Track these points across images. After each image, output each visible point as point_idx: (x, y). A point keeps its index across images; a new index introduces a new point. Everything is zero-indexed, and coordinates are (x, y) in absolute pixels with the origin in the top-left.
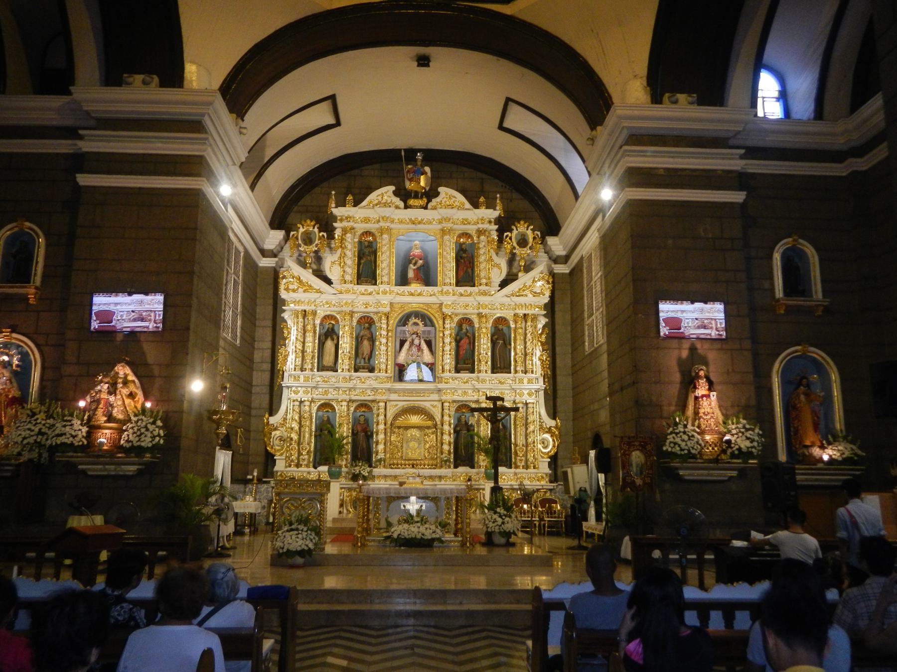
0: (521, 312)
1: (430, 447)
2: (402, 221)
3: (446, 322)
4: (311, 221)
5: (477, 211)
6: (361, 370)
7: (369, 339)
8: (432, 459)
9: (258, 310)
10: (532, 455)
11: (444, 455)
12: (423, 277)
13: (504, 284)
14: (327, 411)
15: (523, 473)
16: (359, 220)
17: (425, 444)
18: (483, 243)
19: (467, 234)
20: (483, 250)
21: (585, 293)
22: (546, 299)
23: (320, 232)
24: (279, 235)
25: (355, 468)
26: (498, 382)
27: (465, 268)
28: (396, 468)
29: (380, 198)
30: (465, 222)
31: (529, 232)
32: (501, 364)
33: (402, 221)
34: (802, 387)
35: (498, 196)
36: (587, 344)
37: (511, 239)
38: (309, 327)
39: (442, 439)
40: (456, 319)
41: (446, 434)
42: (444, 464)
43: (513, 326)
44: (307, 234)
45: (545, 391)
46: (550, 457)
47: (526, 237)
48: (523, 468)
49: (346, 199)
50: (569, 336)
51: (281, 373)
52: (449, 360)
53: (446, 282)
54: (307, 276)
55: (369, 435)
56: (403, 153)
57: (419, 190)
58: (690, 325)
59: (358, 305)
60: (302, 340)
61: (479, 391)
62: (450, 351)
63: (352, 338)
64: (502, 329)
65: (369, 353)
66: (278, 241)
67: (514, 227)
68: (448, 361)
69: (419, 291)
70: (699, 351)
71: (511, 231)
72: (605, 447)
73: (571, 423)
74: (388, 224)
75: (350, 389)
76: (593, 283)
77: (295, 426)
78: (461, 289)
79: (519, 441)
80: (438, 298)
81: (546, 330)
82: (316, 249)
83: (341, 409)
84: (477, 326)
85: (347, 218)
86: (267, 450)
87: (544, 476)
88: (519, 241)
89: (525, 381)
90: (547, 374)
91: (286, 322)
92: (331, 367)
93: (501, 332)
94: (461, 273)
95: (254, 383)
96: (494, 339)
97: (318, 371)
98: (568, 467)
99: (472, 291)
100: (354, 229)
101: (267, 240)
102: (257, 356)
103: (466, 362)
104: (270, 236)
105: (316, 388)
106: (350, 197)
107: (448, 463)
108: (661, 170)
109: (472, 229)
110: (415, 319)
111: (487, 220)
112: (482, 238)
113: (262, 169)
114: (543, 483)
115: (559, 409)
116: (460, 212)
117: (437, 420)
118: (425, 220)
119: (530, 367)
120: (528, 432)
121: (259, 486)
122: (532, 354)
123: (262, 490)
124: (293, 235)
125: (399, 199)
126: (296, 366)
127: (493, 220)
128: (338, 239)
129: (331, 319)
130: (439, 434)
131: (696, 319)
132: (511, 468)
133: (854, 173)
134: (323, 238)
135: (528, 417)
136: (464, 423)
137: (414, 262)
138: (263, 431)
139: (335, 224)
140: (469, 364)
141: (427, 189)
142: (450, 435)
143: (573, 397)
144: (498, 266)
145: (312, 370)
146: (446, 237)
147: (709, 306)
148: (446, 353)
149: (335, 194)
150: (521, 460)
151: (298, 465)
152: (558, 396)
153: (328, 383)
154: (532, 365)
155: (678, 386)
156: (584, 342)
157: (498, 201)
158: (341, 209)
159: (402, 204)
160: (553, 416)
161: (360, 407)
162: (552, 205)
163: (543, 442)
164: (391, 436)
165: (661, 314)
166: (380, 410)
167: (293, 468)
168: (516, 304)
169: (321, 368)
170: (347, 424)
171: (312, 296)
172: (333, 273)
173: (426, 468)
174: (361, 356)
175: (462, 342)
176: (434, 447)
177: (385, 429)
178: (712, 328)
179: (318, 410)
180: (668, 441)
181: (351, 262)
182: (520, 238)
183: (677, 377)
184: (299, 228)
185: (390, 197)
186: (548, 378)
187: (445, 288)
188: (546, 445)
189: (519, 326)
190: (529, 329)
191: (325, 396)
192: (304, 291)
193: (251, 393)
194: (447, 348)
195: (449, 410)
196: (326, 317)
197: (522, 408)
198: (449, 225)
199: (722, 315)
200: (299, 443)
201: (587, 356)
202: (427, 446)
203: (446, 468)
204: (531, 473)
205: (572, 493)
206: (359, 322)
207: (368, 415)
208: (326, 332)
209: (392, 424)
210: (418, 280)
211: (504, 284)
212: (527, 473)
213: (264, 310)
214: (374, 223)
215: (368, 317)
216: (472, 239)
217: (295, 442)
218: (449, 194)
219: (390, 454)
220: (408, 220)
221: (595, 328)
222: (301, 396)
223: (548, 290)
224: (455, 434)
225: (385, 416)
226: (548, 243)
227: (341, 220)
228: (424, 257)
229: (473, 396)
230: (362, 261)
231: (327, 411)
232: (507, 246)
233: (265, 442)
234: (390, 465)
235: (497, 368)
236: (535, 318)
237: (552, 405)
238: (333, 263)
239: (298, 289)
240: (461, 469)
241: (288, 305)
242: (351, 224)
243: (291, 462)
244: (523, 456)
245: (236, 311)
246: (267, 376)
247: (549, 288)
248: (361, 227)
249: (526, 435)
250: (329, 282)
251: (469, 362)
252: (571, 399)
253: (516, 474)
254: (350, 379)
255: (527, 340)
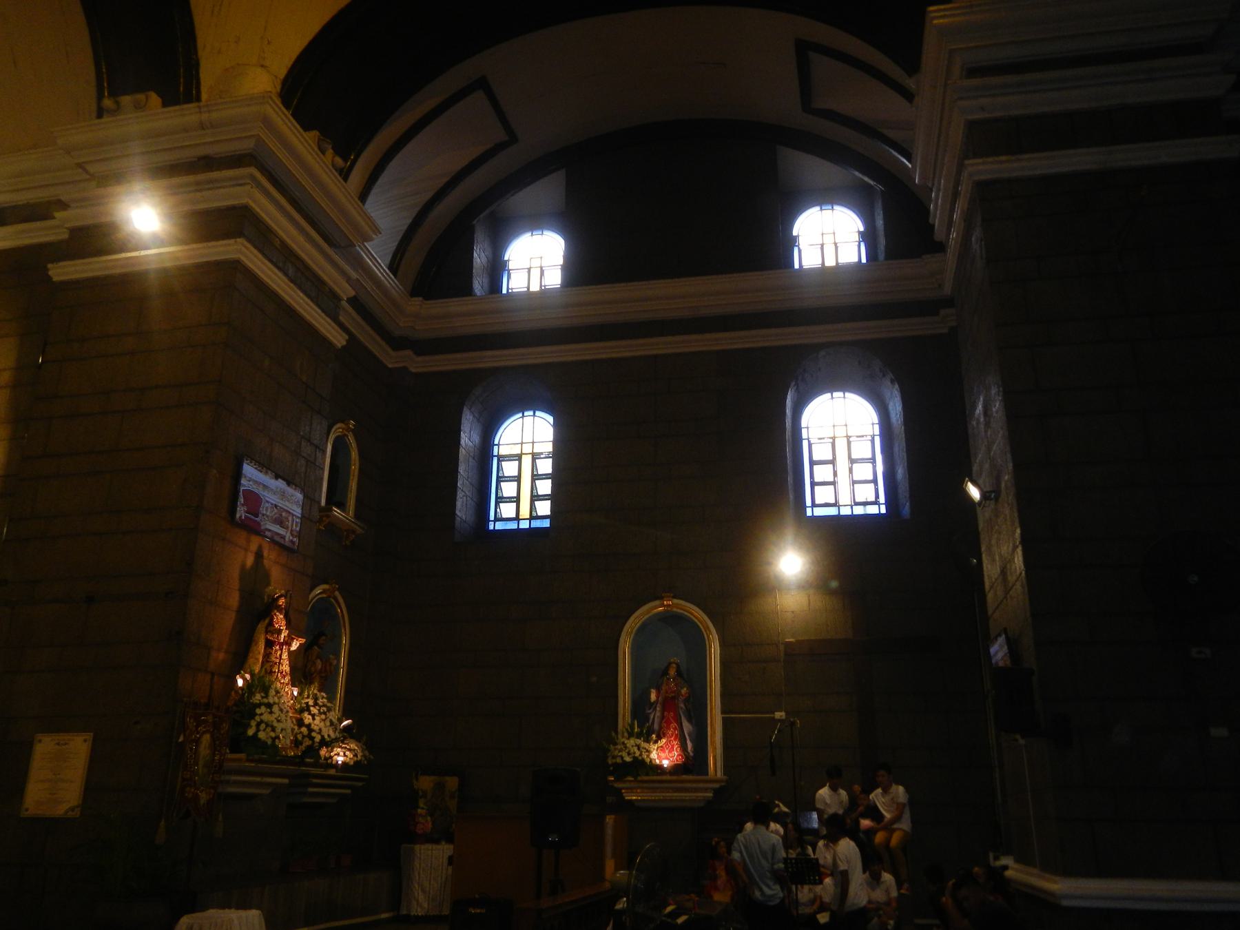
34: (316, 648)
58: (268, 513)
70: (266, 562)
108: (277, 239)
131: (276, 506)
133: (405, 369)
147: (290, 490)
155: (233, 615)
165: (243, 481)
178: (287, 528)
180: (258, 718)
183: (234, 600)
199: (298, 511)
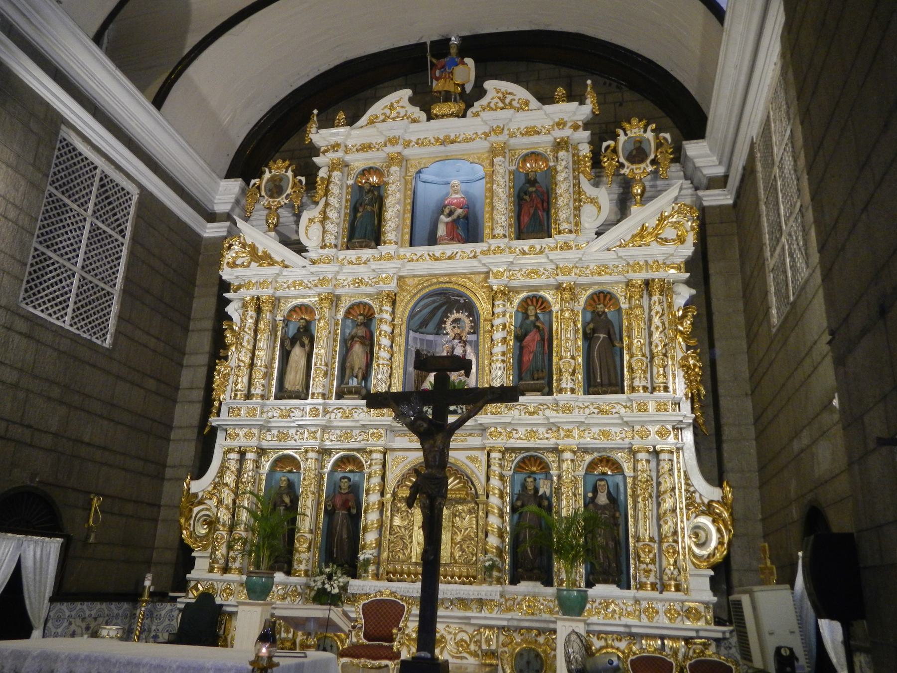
0: (638, 277)
1: (463, 540)
2: (423, 143)
3: (496, 303)
4: (284, 161)
5: (549, 108)
6: (346, 396)
7: (362, 343)
8: (467, 563)
9: (194, 305)
10: (672, 561)
11: (489, 556)
12: (463, 236)
14: (290, 472)
15: (652, 600)
16: (354, 150)
17: (454, 534)
18: (564, 163)
19: (532, 153)
20: (564, 175)
21: (764, 208)
22: (688, 250)
23: (295, 176)
24: (235, 185)
25: (317, 578)
26: (596, 411)
27: (532, 211)
28: (399, 581)
29: (387, 111)
31: (650, 135)
33: (423, 143)
35: (589, 82)
36: (774, 311)
37: (615, 151)
38: (261, 325)
39: (486, 524)
40: (518, 299)
41: (493, 513)
42: (488, 573)
43: (624, 306)
44: (275, 181)
45: (696, 426)
46: (714, 567)
47: (644, 146)
48: (653, 589)
49: (334, 120)
50: (741, 319)
51: (216, 404)
53: (496, 233)
54: (269, 244)
56: (428, 43)
57: (452, 89)
59: (345, 283)
60: (250, 347)
61: (559, 430)
62: (503, 354)
63: (335, 340)
64: (604, 312)
65: (364, 368)
66: (234, 196)
67: (620, 132)
68: (500, 373)
69: (449, 253)
71: (615, 137)
72: (835, 530)
73: (756, 494)
74: (398, 148)
75: (325, 429)
76: (776, 170)
77: (227, 496)
78: (525, 244)
79: (641, 531)
80: (480, 261)
81: (693, 311)
82: (287, 202)
83: (309, 464)
84: (555, 308)
85: (333, 147)
86: (182, 540)
87: (702, 608)
88: (631, 153)
89: (651, 407)
90: (699, 394)
91: (230, 319)
92: (298, 392)
93: (603, 317)
94: (525, 219)
95: (176, 423)
96: (588, 332)
97: (276, 398)
98: (745, 592)
99: (544, 246)
100: (347, 166)
101: (217, 197)
102: (186, 378)
103: (536, 376)
104: (221, 189)
105: (265, 428)
106: (341, 116)
107: (495, 574)
109: (543, 143)
110: (458, 312)
111: (569, 124)
112: (562, 154)
113: (180, 63)
114: (701, 624)
115: (728, 465)
116: (521, 114)
117: (478, 486)
118: (462, 136)
119: (661, 379)
120: (662, 511)
121: (159, 606)
122: (665, 355)
123: (163, 613)
124: (255, 184)
125: (418, 109)
126: (236, 390)
127: (580, 123)
128: (323, 183)
129: (306, 313)
130: (481, 513)
132: (629, 588)
134: (298, 184)
135: (661, 480)
136: (532, 492)
137: (447, 211)
138: (178, 507)
139: (315, 159)
140: (543, 379)
141: (469, 88)
142: (501, 515)
143: (757, 439)
144: (593, 201)
145: (263, 397)
146: (497, 160)
148: (495, 358)
149: (318, 115)
150: (647, 572)
151: (226, 570)
152: (724, 438)
153: (289, 419)
154: (665, 375)
156: (768, 309)
157: (589, 89)
158: (323, 132)
159: (423, 116)
160: (716, 476)
161: (344, 463)
162: (693, 93)
163: (696, 531)
164: (392, 516)
166: (374, 467)
167: (217, 575)
168: (628, 264)
169: (282, 393)
170: (313, 493)
171: (268, 272)
172: (310, 235)
173: (456, 583)
174: (348, 372)
175: (528, 338)
176: (472, 539)
177: (382, 505)
179: (272, 470)
181: (336, 215)
182: (631, 147)
184: (264, 173)
185: (402, 107)
186: (700, 400)
187: (495, 243)
188: (703, 540)
189: (635, 302)
190: (657, 308)
191: (282, 442)
192: (260, 265)
193: (168, 440)
194: (498, 349)
195: (500, 465)
196: (297, 309)
197: (648, 461)
200: (232, 528)
201: (776, 335)
202: (459, 538)
203: (490, 584)
204: (670, 600)
205: (758, 663)
206: (348, 312)
207: (354, 478)
208: (295, 335)
209: (394, 495)
210: (452, 239)
212: (661, 600)
213: (203, 306)
214: (378, 149)
215: (365, 305)
216: (546, 160)
217: (224, 525)
218: (503, 90)
219: (389, 552)
220: (433, 141)
221: (788, 260)
222: (242, 442)
223: (692, 233)
224: (516, 516)
225: (383, 478)
226: (688, 153)
227: (324, 153)
229: (547, 439)
230: (359, 215)
231: (290, 472)
233: (181, 526)
234: (388, 573)
235: (595, 386)
236: (666, 288)
237: (715, 459)
238: (311, 220)
239: (249, 263)
240: (525, 587)
241: (235, 291)
242: (340, 154)
243: (213, 562)
244: (653, 561)
245: (102, 285)
246: (196, 410)
247: (692, 229)
248: (359, 161)
249: (659, 518)
250: (299, 248)
251: (541, 375)
252: (754, 442)
253: (637, 601)
254: (326, 412)
255: (653, 328)
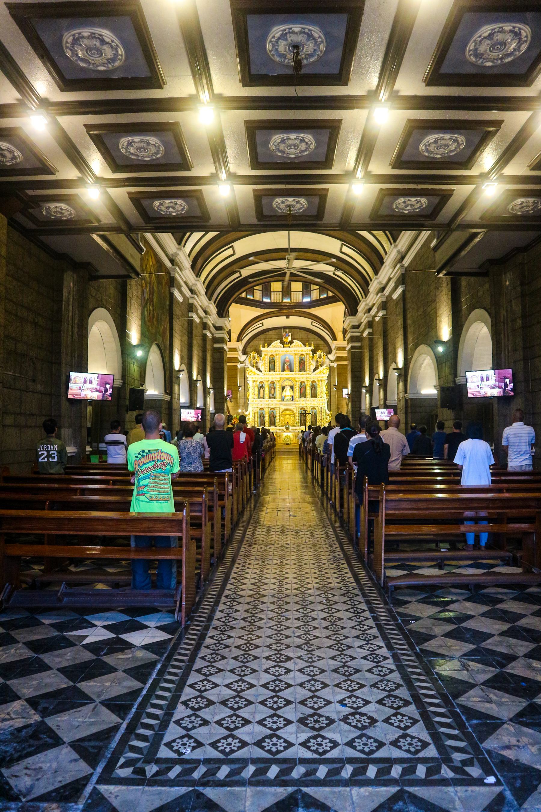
13: (314, 370)
24: (245, 356)
30: (302, 351)
32: (314, 395)
52: (298, 394)
54: (254, 369)
55: (274, 417)
78: (301, 373)
83: (266, 410)
109: (304, 353)
160: (330, 410)
169: (260, 398)
171: (256, 376)
172: (262, 368)
198: (297, 352)
211: (314, 370)
228: (289, 361)
232: (315, 358)
248: (270, 354)
250: (261, 371)
